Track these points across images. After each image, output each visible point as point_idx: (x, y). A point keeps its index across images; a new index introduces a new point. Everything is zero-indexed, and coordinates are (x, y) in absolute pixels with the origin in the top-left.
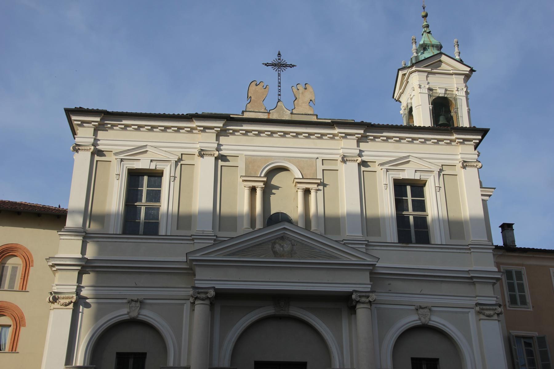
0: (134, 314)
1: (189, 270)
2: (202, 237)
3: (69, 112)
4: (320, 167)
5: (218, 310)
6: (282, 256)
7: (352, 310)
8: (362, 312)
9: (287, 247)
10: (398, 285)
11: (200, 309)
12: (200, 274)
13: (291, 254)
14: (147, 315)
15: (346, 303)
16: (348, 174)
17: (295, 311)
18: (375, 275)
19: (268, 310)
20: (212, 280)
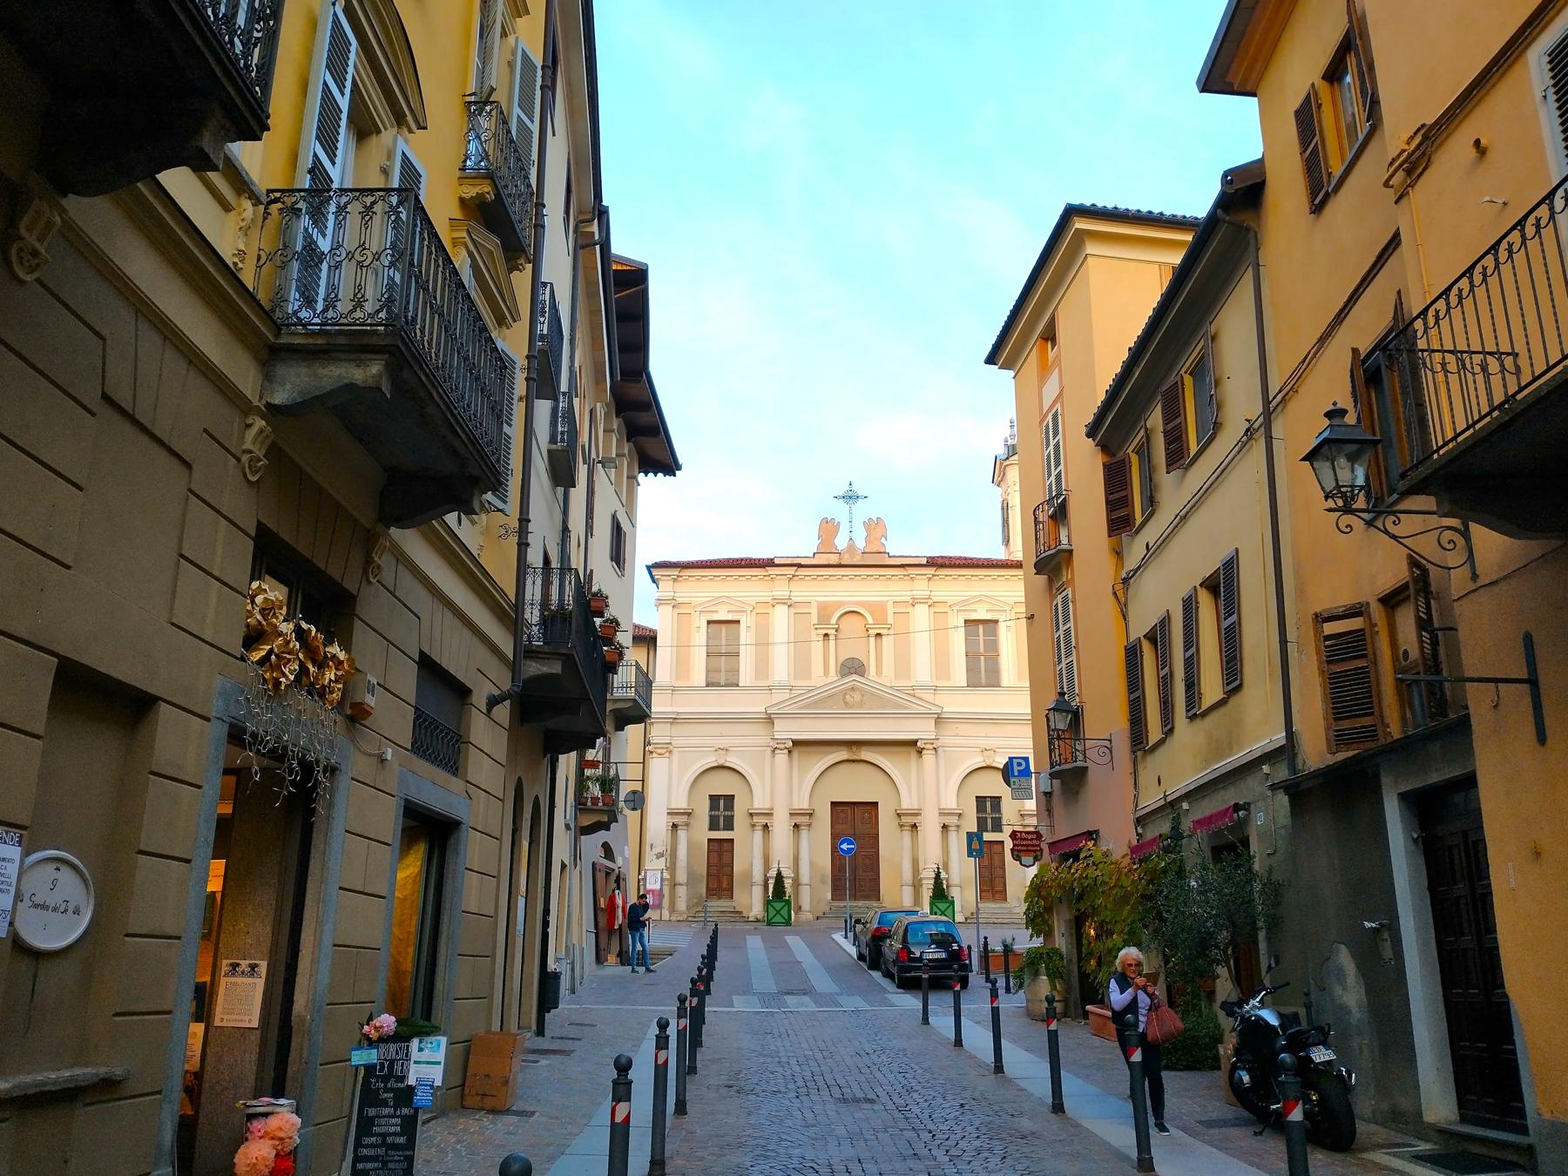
0: (721, 762)
1: (769, 720)
2: (781, 687)
3: (649, 568)
4: (890, 609)
5: (795, 754)
6: (852, 707)
7: (920, 752)
8: (928, 757)
9: (857, 697)
10: (964, 729)
11: (782, 757)
12: (779, 725)
13: (861, 704)
14: (732, 761)
15: (911, 745)
16: (921, 617)
17: (866, 754)
18: (939, 720)
19: (843, 754)
20: (789, 730)
